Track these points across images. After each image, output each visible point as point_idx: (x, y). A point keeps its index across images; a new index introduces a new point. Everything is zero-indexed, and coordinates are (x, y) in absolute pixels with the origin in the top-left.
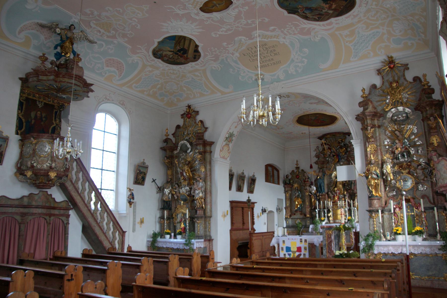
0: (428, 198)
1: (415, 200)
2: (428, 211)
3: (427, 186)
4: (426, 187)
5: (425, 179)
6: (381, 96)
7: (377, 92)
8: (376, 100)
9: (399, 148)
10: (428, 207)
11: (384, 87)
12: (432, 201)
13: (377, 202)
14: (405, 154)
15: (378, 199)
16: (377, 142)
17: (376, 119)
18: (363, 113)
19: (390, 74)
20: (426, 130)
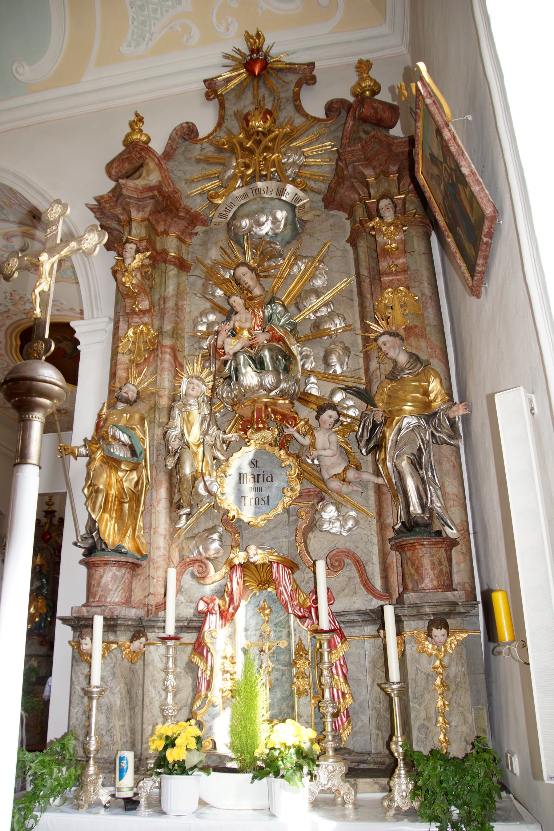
0: (360, 565)
1: (297, 575)
2: (356, 631)
3: (358, 509)
4: (353, 513)
5: (351, 474)
6: (208, 161)
7: (196, 151)
8: (188, 176)
9: (242, 329)
10: (358, 612)
11: (222, 136)
12: (378, 584)
13: (115, 578)
14: (266, 354)
15: (121, 564)
16: (162, 318)
17: (174, 231)
18: (116, 193)
19: (249, 94)
20: (364, 272)
